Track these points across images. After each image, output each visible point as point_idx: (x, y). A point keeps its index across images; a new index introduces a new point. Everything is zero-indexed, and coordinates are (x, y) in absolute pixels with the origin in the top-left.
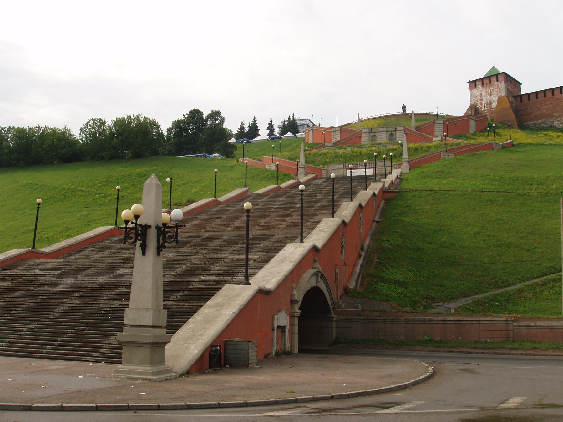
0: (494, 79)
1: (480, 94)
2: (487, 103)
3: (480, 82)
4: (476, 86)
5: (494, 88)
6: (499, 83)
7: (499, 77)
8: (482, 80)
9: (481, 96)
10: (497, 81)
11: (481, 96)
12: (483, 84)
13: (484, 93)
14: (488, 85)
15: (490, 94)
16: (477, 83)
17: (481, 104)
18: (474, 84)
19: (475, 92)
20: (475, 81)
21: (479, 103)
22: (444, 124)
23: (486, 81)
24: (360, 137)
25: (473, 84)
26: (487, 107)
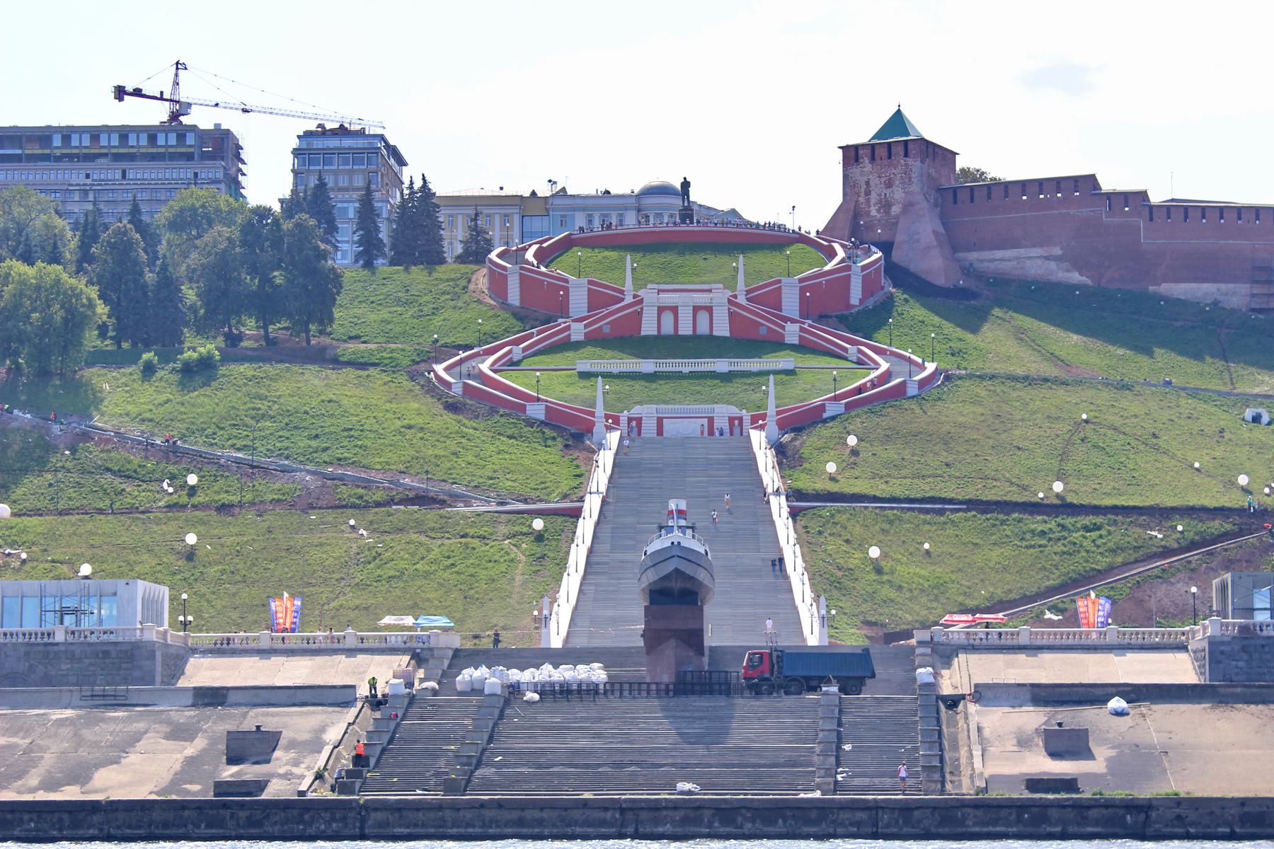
0: (901, 150)
1: (865, 179)
2: (880, 201)
3: (868, 151)
4: (857, 159)
5: (897, 172)
6: (910, 161)
7: (910, 146)
8: (871, 148)
9: (868, 183)
10: (906, 155)
11: (868, 183)
12: (873, 159)
13: (874, 180)
14: (886, 162)
15: (889, 184)
16: (861, 152)
17: (868, 201)
18: (853, 153)
19: (855, 171)
20: (856, 148)
21: (862, 199)
22: (802, 291)
23: (881, 152)
24: (640, 314)
25: (852, 154)
26: (878, 211)
